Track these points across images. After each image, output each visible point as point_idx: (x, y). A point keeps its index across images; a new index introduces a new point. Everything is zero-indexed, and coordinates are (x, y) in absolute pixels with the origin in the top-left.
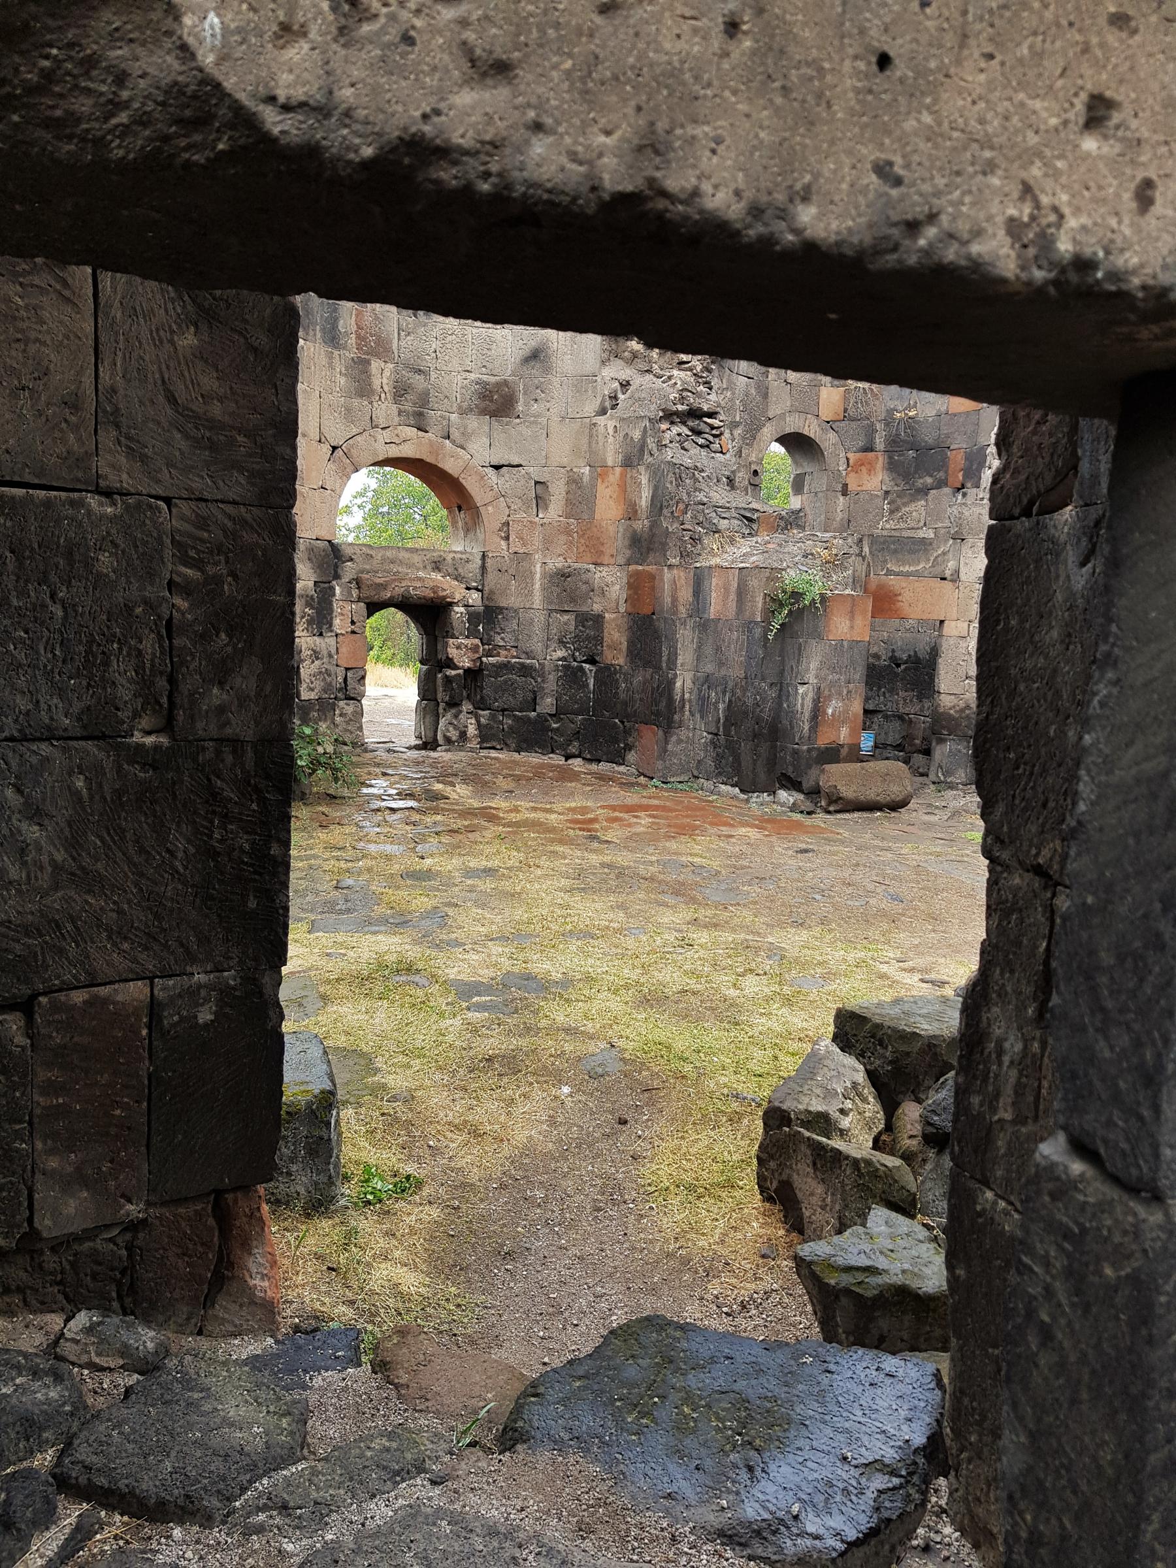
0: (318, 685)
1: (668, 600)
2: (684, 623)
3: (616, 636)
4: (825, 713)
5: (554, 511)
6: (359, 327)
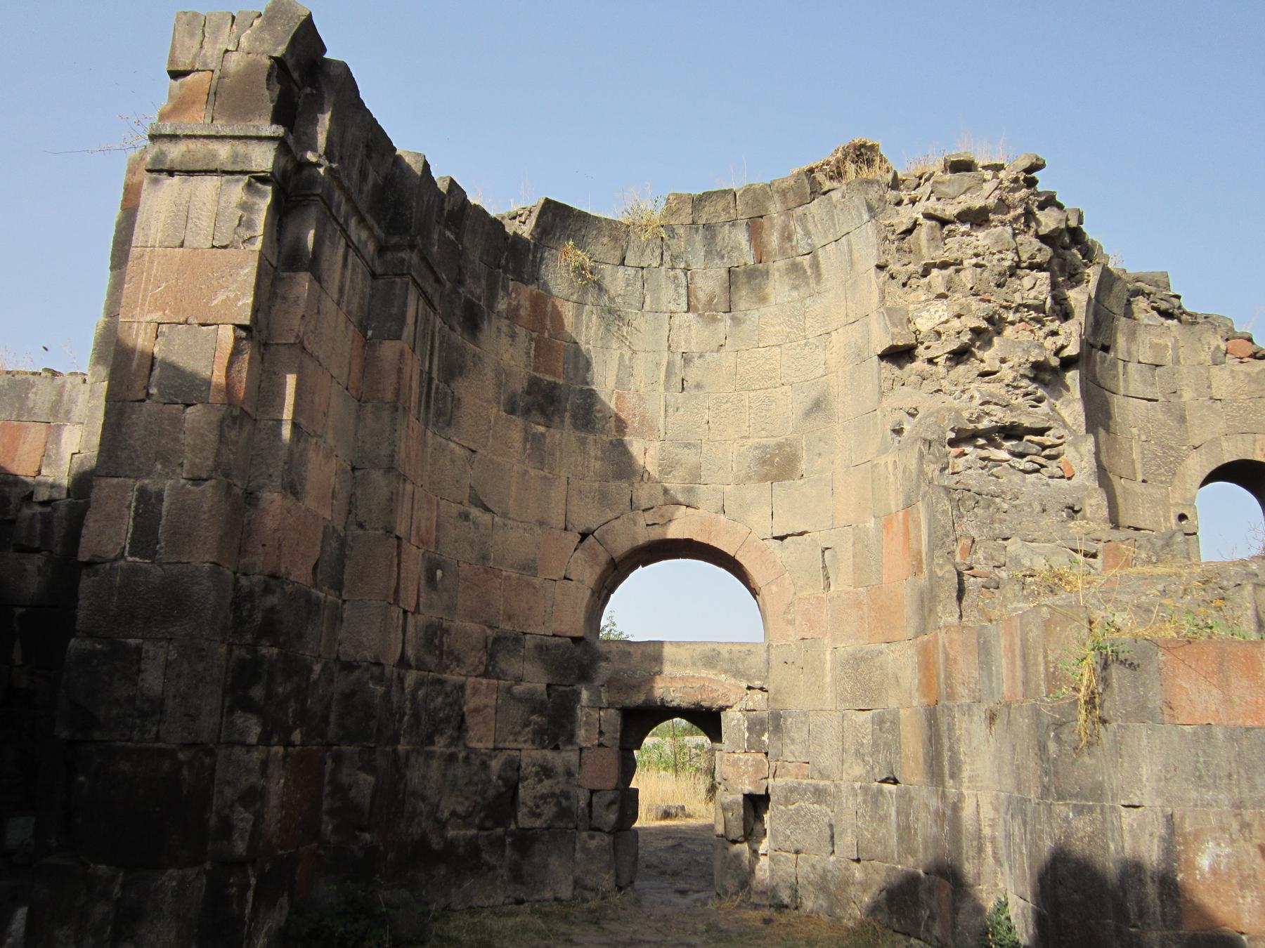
0: (549, 811)
2: (968, 710)
5: (842, 583)
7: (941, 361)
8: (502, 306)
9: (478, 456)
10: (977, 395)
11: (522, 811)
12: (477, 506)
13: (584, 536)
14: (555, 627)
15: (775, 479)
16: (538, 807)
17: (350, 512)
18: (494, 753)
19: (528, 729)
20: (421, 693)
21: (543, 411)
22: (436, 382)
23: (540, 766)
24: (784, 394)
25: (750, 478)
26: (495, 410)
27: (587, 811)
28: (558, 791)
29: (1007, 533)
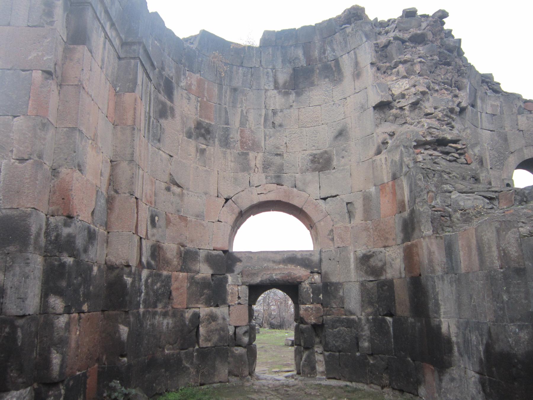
1: (426, 261)
3: (402, 295)
6: (242, 137)
7: (407, 108)
9: (173, 159)
10: (426, 124)
11: (201, 339)
12: (174, 185)
13: (227, 200)
15: (320, 170)
17: (110, 184)
18: (186, 310)
19: (203, 297)
21: (205, 139)
22: (152, 119)
23: (209, 315)
26: (181, 136)
27: (233, 336)
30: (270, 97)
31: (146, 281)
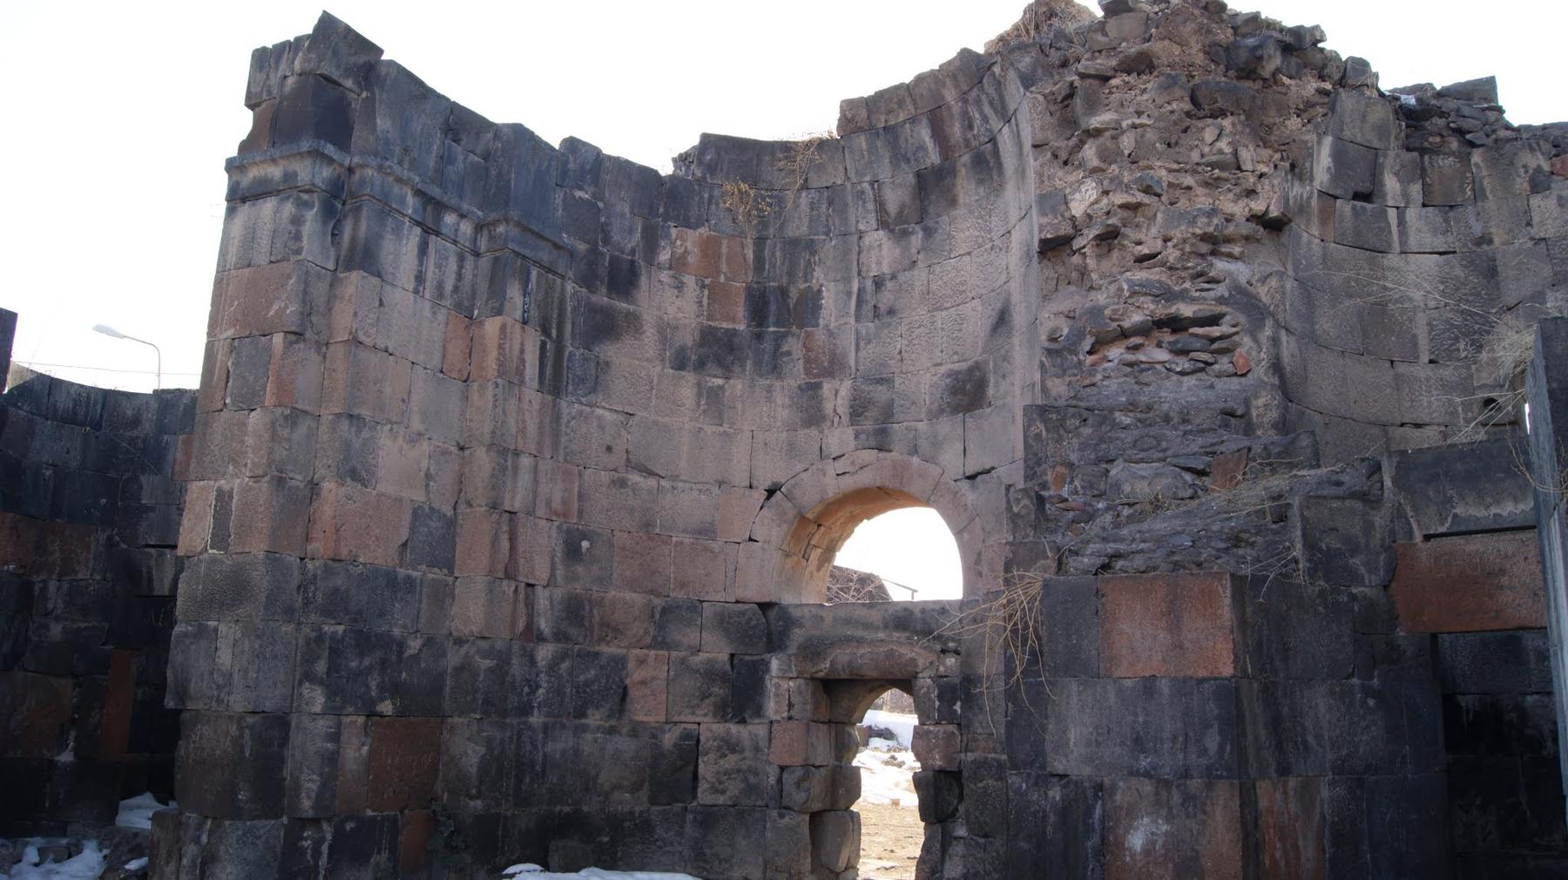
0: (734, 788)
4: (1120, 844)
6: (808, 350)
8: (664, 256)
9: (633, 421)
11: (703, 786)
13: (771, 492)
14: (740, 593)
16: (720, 783)
18: (667, 727)
19: (707, 701)
20: (565, 666)
21: (720, 362)
24: (974, 310)
25: (942, 411)
28: (744, 767)
29: (1113, 453)
30: (870, 248)
31: (553, 667)
